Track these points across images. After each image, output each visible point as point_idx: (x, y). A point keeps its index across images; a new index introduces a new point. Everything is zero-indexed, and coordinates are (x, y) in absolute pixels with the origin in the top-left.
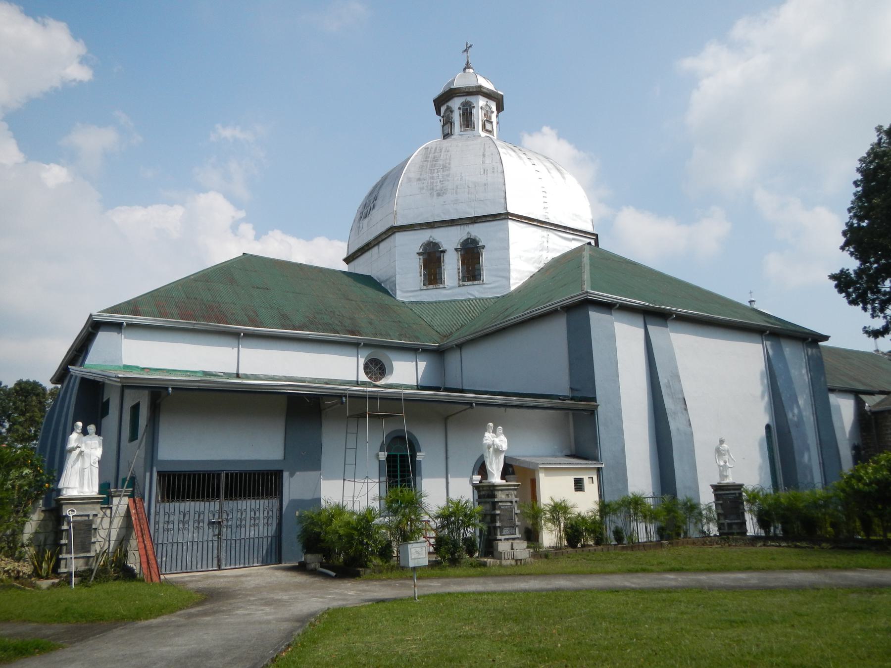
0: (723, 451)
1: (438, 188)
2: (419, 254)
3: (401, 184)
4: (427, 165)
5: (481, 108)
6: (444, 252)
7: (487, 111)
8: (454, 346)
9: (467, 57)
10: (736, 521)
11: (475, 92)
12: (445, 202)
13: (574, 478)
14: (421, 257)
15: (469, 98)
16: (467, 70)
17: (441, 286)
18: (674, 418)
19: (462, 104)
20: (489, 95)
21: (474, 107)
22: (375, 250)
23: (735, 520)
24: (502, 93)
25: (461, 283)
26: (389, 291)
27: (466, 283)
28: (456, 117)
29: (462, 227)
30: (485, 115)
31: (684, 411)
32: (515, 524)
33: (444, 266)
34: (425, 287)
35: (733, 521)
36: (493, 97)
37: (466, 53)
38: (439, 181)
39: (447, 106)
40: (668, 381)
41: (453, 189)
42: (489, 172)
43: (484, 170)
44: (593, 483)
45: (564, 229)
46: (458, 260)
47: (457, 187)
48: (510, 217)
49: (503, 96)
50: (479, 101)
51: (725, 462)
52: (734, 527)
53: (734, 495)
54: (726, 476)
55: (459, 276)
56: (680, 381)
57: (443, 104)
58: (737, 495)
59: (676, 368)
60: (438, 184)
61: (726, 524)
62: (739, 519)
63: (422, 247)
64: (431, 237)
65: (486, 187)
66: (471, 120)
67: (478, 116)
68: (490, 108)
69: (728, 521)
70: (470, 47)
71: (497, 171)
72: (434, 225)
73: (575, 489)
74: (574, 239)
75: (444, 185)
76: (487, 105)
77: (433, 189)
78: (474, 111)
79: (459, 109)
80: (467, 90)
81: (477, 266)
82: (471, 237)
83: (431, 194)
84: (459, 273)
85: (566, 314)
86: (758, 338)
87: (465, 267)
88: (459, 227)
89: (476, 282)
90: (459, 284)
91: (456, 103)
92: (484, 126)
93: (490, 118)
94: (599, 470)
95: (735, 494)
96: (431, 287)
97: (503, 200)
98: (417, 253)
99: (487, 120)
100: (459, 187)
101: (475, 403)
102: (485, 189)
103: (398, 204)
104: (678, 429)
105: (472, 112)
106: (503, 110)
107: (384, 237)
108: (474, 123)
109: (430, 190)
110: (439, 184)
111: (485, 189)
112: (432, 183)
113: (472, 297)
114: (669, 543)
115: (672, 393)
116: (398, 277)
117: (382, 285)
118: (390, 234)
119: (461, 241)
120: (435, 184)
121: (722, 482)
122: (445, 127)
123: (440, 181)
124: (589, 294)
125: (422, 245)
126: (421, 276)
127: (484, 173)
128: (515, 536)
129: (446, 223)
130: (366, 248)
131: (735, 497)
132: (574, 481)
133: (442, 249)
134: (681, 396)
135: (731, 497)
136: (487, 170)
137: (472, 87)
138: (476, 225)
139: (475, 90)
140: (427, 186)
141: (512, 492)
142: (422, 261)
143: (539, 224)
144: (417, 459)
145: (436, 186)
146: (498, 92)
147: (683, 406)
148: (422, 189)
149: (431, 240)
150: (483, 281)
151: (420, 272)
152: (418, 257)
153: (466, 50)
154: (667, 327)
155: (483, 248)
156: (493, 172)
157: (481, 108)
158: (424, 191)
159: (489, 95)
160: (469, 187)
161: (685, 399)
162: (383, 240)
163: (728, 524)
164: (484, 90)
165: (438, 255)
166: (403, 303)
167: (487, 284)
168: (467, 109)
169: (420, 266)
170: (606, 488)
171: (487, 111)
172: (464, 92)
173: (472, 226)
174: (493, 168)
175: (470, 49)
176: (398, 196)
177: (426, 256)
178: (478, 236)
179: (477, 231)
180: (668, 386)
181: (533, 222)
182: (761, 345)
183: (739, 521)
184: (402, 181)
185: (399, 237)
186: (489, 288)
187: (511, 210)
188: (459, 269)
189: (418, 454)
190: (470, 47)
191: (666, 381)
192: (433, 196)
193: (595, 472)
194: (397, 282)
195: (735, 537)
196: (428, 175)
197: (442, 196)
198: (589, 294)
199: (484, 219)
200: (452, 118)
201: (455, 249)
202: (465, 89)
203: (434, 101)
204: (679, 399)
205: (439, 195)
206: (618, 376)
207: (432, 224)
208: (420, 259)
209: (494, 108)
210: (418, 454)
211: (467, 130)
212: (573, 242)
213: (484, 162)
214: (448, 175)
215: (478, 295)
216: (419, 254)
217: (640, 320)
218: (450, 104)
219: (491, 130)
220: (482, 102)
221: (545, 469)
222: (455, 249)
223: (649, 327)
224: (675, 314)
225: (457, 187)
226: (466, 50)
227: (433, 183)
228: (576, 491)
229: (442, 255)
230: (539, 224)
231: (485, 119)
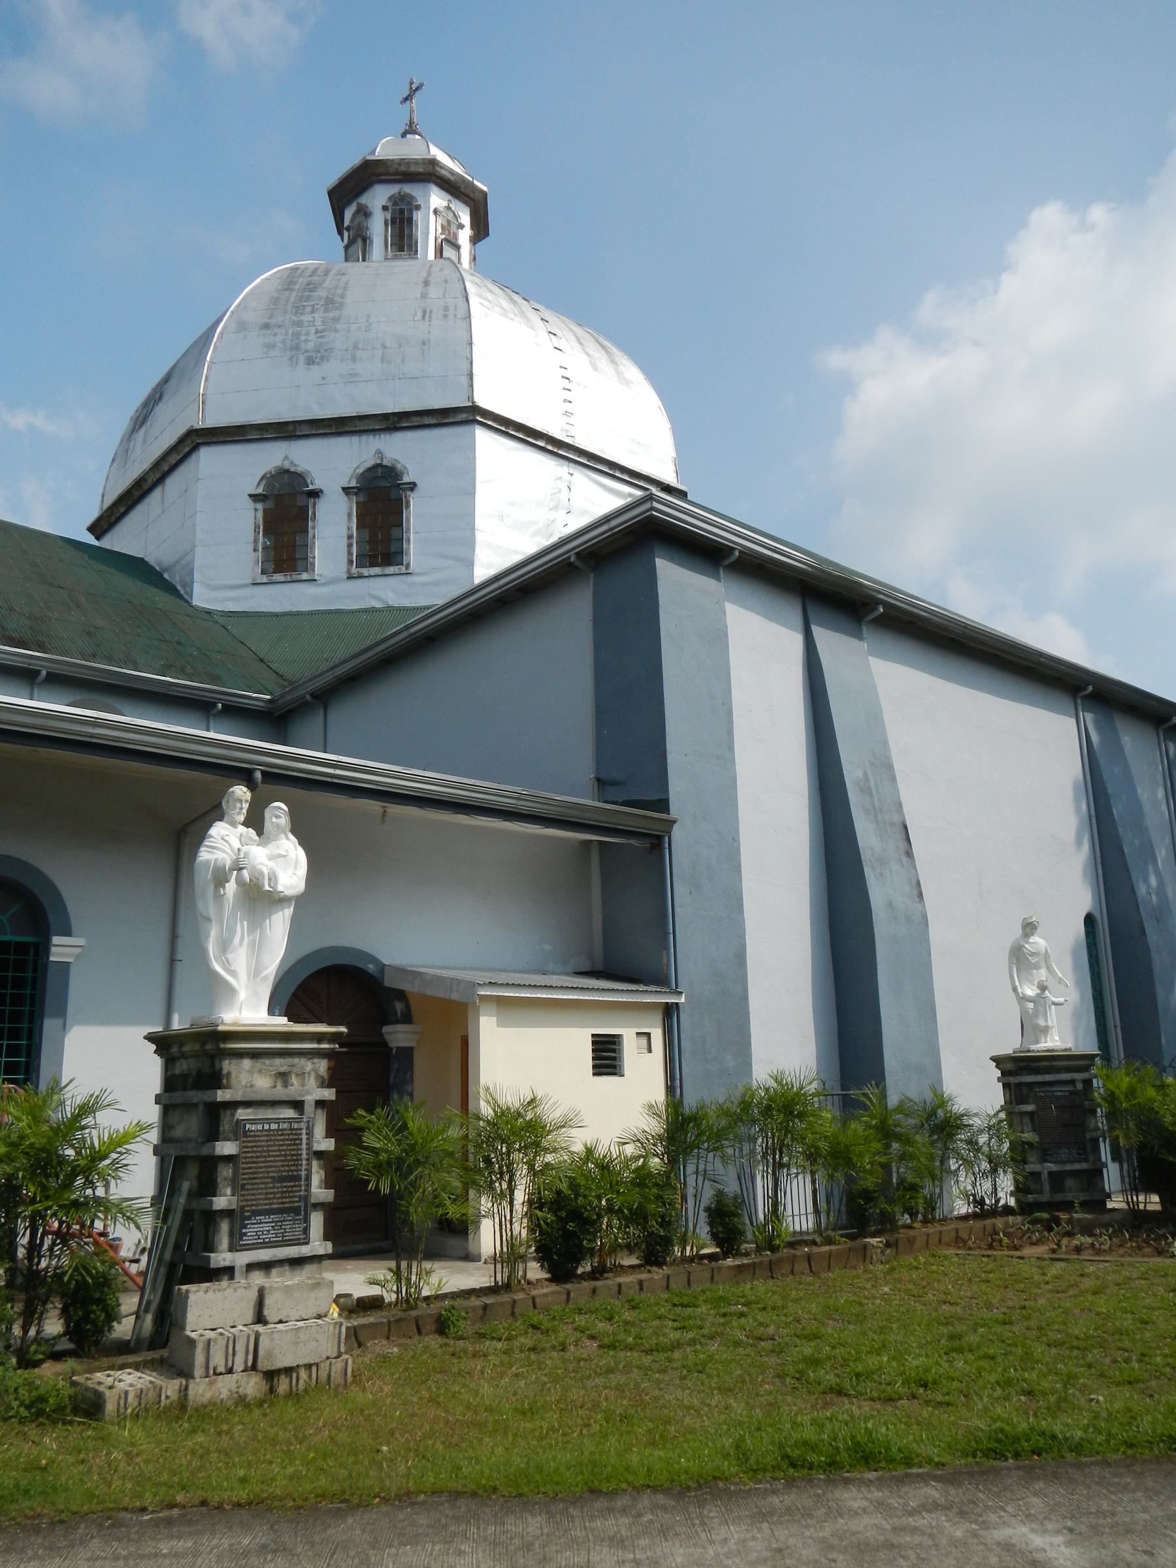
0: (1034, 954)
1: (311, 345)
2: (254, 497)
3: (222, 333)
4: (289, 298)
5: (436, 212)
6: (316, 494)
7: (449, 222)
8: (308, 697)
9: (412, 111)
10: (1077, 1166)
11: (420, 174)
12: (324, 378)
13: (593, 1035)
14: (260, 506)
15: (408, 189)
16: (409, 136)
17: (305, 576)
18: (881, 875)
19: (390, 198)
20: (455, 188)
21: (418, 208)
22: (155, 497)
23: (1071, 1162)
24: (485, 188)
25: (354, 570)
26: (179, 588)
27: (365, 572)
28: (378, 227)
29: (364, 438)
30: (443, 227)
31: (905, 859)
32: (306, 1198)
33: (314, 528)
34: (265, 579)
35: (1068, 1167)
36: (463, 193)
37: (408, 102)
38: (313, 330)
39: (359, 205)
40: (865, 774)
41: (347, 350)
42: (434, 316)
43: (424, 312)
44: (650, 1051)
45: (610, 469)
46: (349, 515)
47: (356, 346)
48: (479, 418)
49: (485, 194)
50: (429, 196)
51: (1043, 988)
52: (1070, 1183)
53: (1069, 1088)
54: (1045, 1030)
55: (350, 553)
56: (893, 779)
57: (349, 203)
58: (1080, 1086)
59: (885, 743)
60: (309, 338)
61: (1045, 1175)
62: (1086, 1160)
63: (264, 482)
64: (286, 458)
65: (426, 348)
66: (411, 236)
67: (429, 229)
68: (456, 217)
69: (1053, 1167)
70: (417, 89)
71: (455, 315)
72: (295, 430)
73: (594, 1067)
75: (325, 340)
76: (448, 208)
77: (297, 348)
78: (418, 216)
79: (385, 208)
80: (403, 168)
81: (395, 532)
82: (385, 463)
83: (291, 359)
84: (350, 546)
85: (592, 575)
86: (1066, 701)
87: (366, 535)
88: (355, 439)
89: (391, 570)
90: (349, 571)
91: (378, 197)
92: (439, 252)
93: (456, 236)
94: (669, 1012)
95: (1072, 1082)
96: (279, 577)
97: (464, 380)
98: (250, 496)
99: (446, 240)
100: (360, 346)
101: (264, 773)
102: (423, 353)
103: (210, 379)
104: (890, 904)
105: (414, 218)
106: (487, 234)
107: (173, 459)
108: (417, 242)
109: (291, 349)
110: (312, 337)
111: (423, 353)
112: (297, 335)
113: (378, 605)
114: (888, 1245)
115: (874, 808)
116: (199, 551)
117: (166, 576)
118: (187, 449)
119: (361, 471)
120: (303, 338)
121: (1033, 1047)
122: (351, 250)
123: (317, 332)
124: (656, 505)
125: (262, 479)
126: (255, 550)
127: (424, 317)
128: (305, 1250)
129: (324, 427)
130: (136, 494)
131: (1071, 1093)
132: (593, 1043)
133: (311, 487)
134: (896, 819)
135: (1060, 1091)
136: (431, 312)
137: (416, 162)
138: (398, 437)
139: (421, 170)
140: (284, 342)
141: (308, 1065)
142: (260, 515)
143: (550, 447)
144: (52, 959)
145: (306, 341)
146: (476, 183)
147: (902, 845)
148: (270, 347)
149: (287, 465)
150: (408, 566)
151: (256, 541)
152: (250, 504)
153: (407, 98)
154: (860, 638)
155: (412, 490)
156: (445, 316)
157: (436, 212)
158: (275, 353)
159: (455, 188)
160: (384, 346)
161: (906, 828)
162: (173, 468)
163: (1051, 1173)
164: (443, 172)
165: (300, 501)
166: (208, 612)
167: (419, 574)
168: (402, 211)
169: (256, 527)
170: (689, 1067)
171: (449, 222)
172: (397, 173)
173: (387, 436)
174: (446, 309)
175: (418, 94)
176: (211, 362)
177: (270, 504)
178: (401, 460)
180: (866, 791)
181: (536, 439)
182: (1074, 721)
183: (1084, 1166)
184: (225, 327)
185: (208, 458)
186: (423, 584)
187: (483, 399)
188: (350, 537)
189: (56, 940)
190: (417, 89)
191: (860, 774)
192: (297, 363)
193: (658, 1017)
194: (197, 564)
195: (1075, 1215)
196: (288, 316)
197: (318, 364)
198: (656, 505)
199: (416, 421)
200: (367, 228)
201: (344, 489)
202: (400, 165)
203: (331, 193)
204: (892, 824)
205: (310, 361)
206: (731, 748)
207: (291, 428)
208: (256, 510)
209: (465, 218)
210: (56, 940)
211: (401, 258)
213: (424, 296)
214: (337, 320)
215: (394, 600)
216: (254, 497)
217: (794, 612)
218: (364, 199)
220: (437, 199)
221: (501, 1002)
222: (344, 489)
223: (818, 631)
224: (885, 603)
225: (356, 346)
226: (407, 98)
227: (298, 335)
228: (594, 1074)
229: (311, 501)
230: (550, 447)
231: (443, 236)
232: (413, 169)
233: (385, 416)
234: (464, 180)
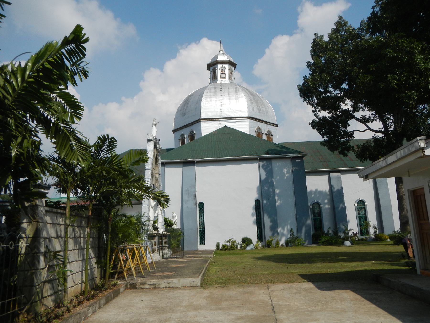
1: (184, 113)
2: (179, 140)
15: (215, 66)
20: (223, 62)
31: (193, 200)
40: (188, 189)
67: (219, 72)
74: (236, 122)
80: (213, 63)
91: (212, 68)
92: (221, 76)
93: (224, 72)
104: (188, 207)
134: (193, 194)
137: (214, 62)
147: (194, 197)
161: (195, 196)
164: (219, 62)
171: (223, 69)
179: (193, 127)
187: (203, 116)
191: (187, 188)
199: (194, 123)
205: (184, 115)
212: (236, 123)
219: (224, 77)
232: (214, 63)
233: (191, 123)
234: (224, 60)
